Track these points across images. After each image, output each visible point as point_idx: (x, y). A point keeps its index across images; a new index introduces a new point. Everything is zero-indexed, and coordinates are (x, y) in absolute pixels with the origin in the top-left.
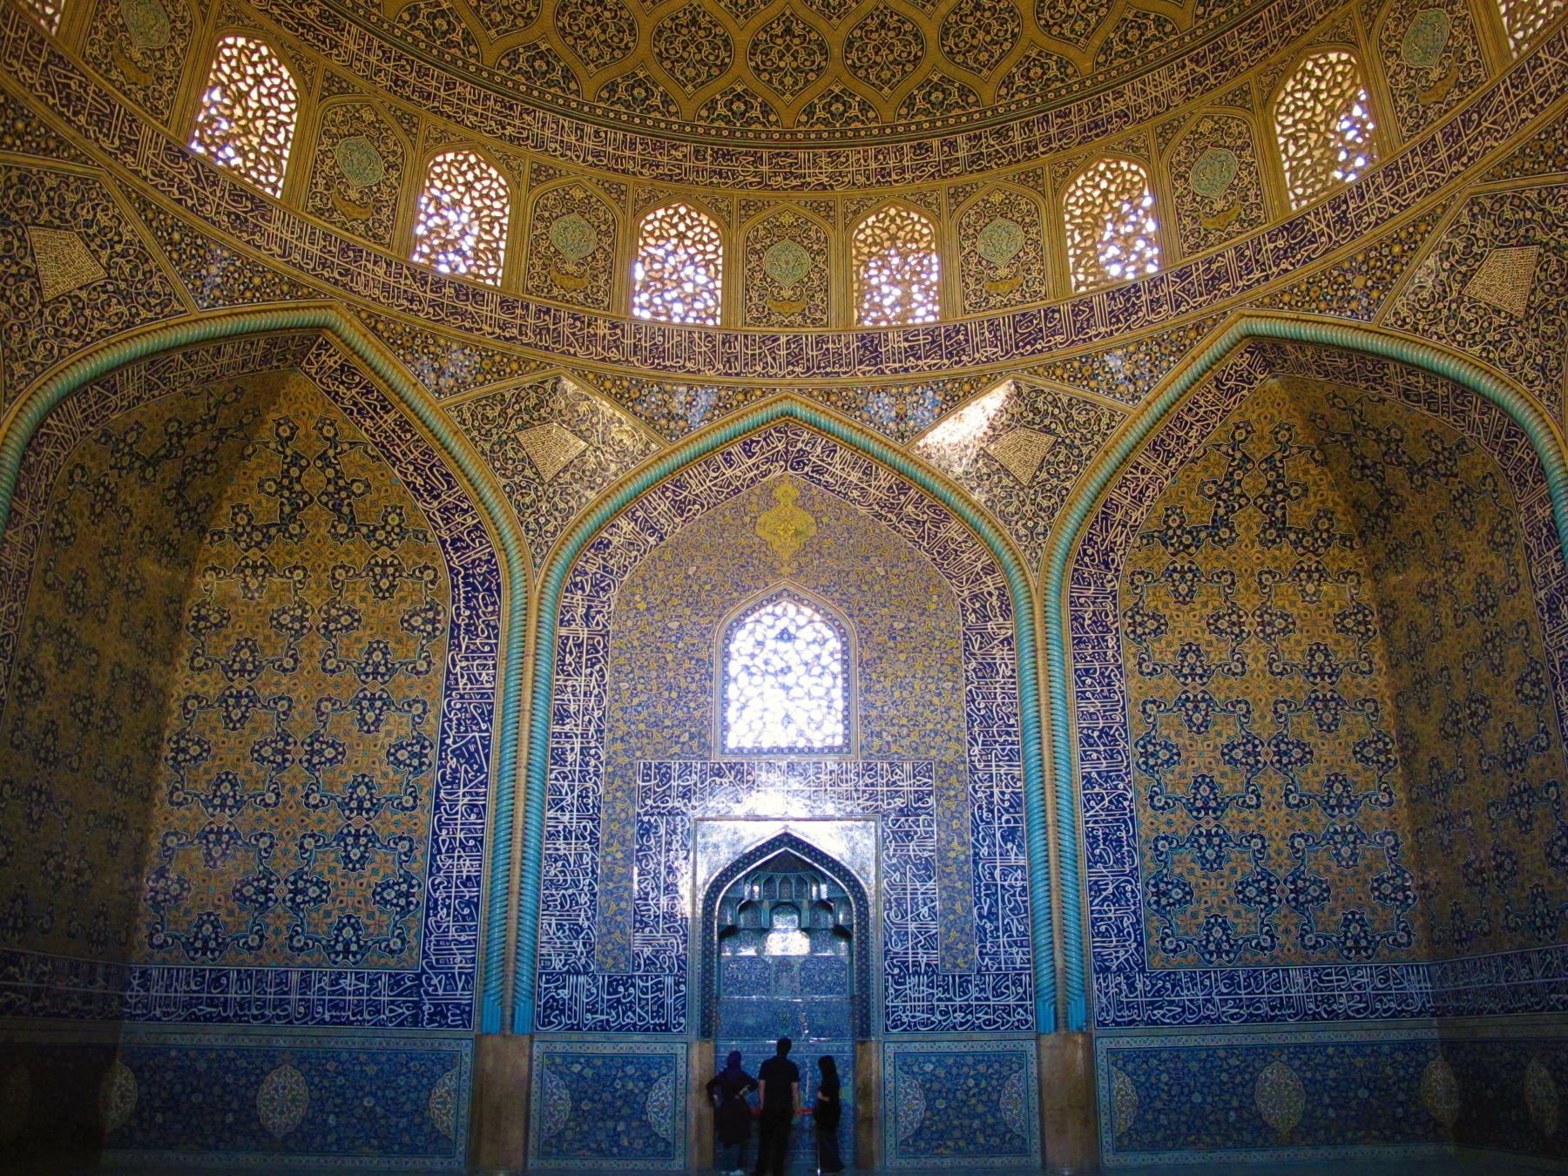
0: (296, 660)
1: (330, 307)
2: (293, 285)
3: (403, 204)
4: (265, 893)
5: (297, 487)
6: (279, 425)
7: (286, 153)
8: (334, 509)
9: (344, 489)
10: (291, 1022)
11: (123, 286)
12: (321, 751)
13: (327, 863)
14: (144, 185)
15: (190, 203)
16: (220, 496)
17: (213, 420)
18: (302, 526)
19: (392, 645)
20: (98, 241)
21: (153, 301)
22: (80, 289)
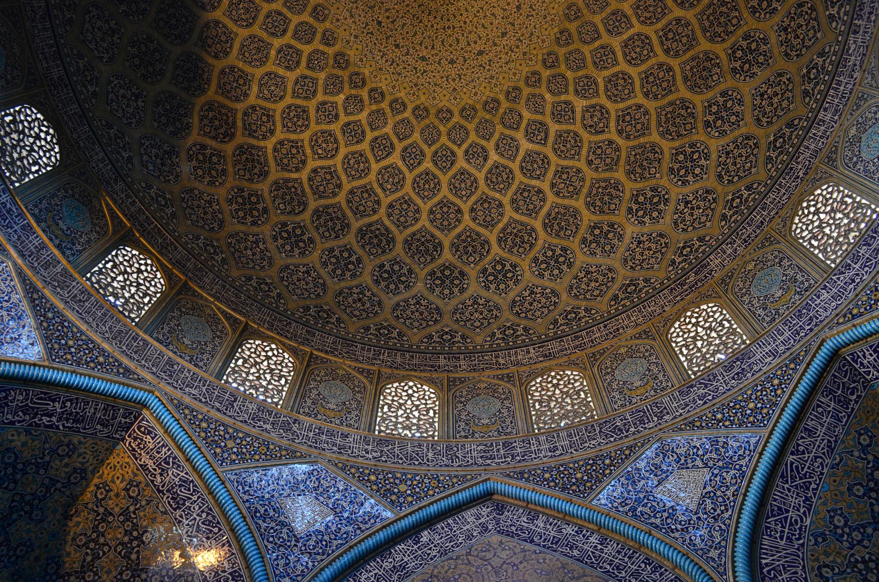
1: (824, 341)
2: (793, 361)
3: (802, 263)
7: (735, 326)
11: (720, 464)
14: (682, 417)
15: (710, 397)
20: (689, 461)
21: (741, 452)
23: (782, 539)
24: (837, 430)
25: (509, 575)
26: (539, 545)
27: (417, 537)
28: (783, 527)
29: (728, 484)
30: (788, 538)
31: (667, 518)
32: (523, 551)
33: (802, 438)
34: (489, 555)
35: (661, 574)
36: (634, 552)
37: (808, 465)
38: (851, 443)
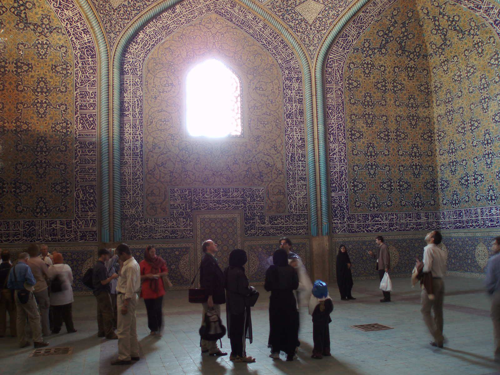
0: (461, 92)
4: (467, 181)
5: (441, 28)
6: (422, 10)
8: (455, 30)
9: (453, 21)
10: (480, 227)
11: (330, 5)
12: (474, 123)
13: (481, 167)
16: (423, 42)
17: (396, 22)
18: (449, 41)
19: (487, 74)
21: (341, 4)
22: (319, 14)
23: (341, 48)
24: (386, 6)
25: (219, 39)
26: (235, 23)
27: (174, 9)
28: (344, 43)
29: (330, 17)
30: (344, 48)
31: (297, 24)
32: (227, 26)
33: (371, 6)
34: (210, 26)
35: (286, 50)
36: (277, 35)
37: (366, 18)
38: (389, 13)
